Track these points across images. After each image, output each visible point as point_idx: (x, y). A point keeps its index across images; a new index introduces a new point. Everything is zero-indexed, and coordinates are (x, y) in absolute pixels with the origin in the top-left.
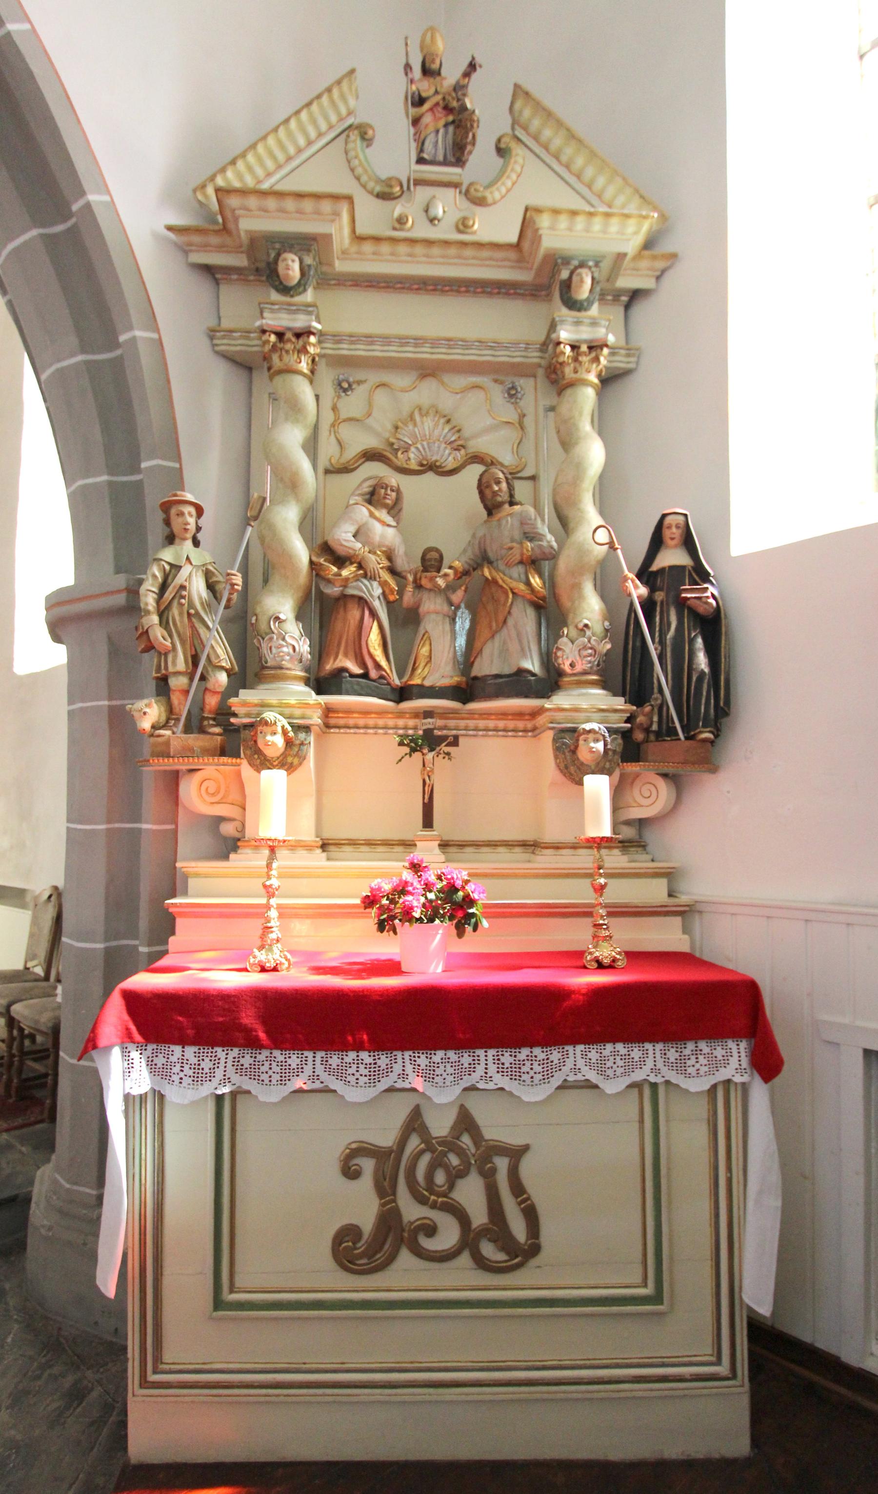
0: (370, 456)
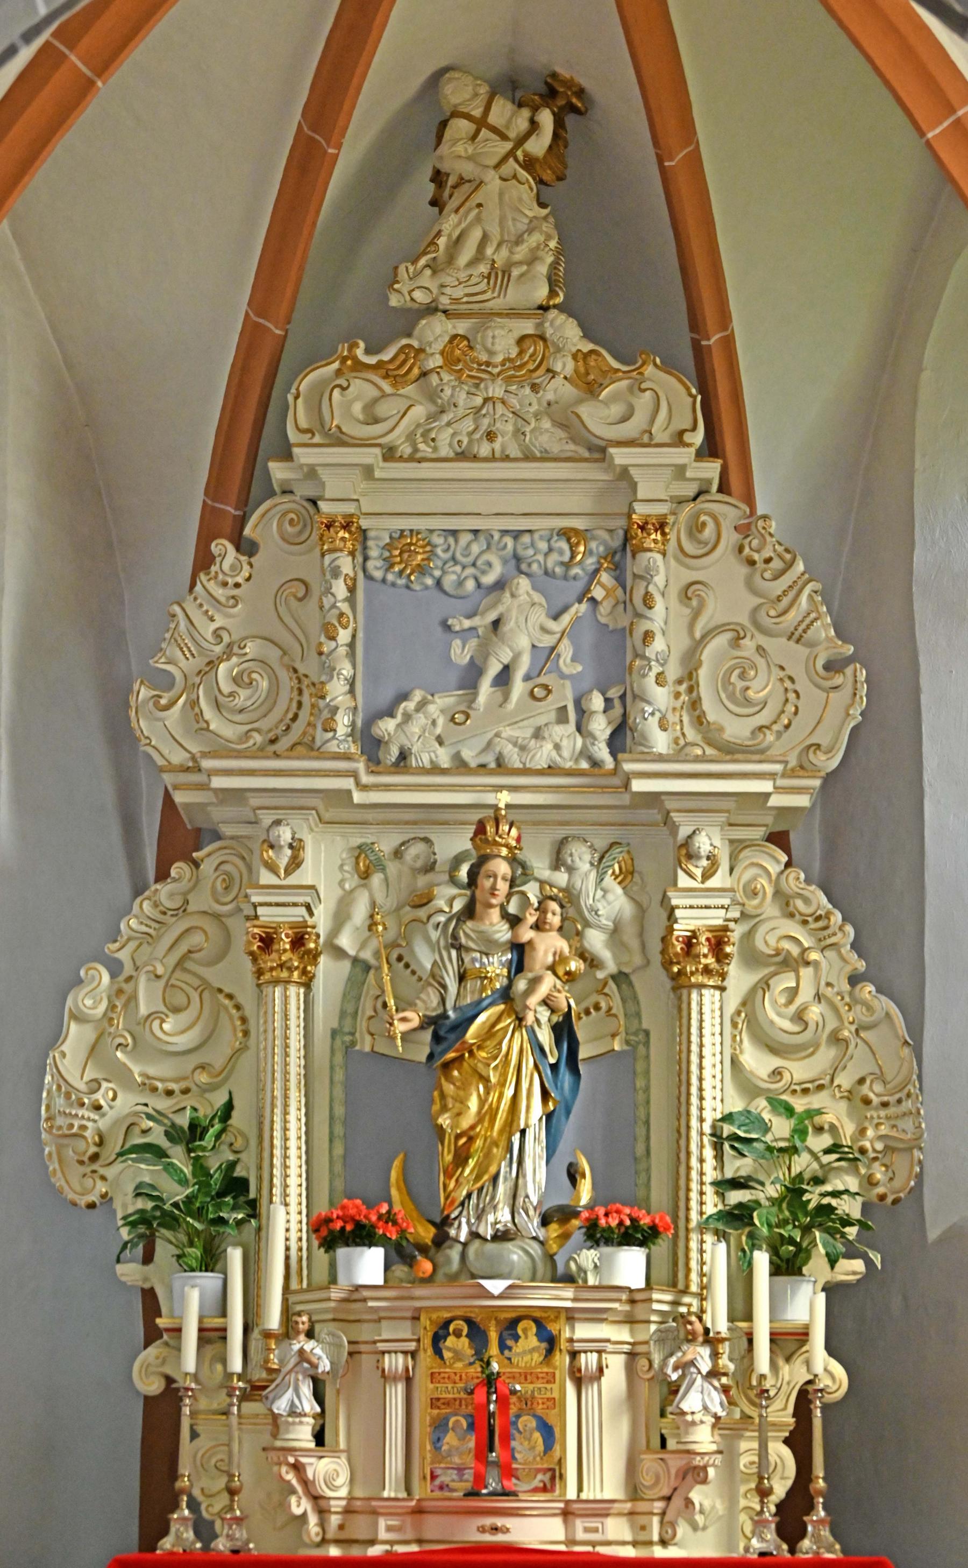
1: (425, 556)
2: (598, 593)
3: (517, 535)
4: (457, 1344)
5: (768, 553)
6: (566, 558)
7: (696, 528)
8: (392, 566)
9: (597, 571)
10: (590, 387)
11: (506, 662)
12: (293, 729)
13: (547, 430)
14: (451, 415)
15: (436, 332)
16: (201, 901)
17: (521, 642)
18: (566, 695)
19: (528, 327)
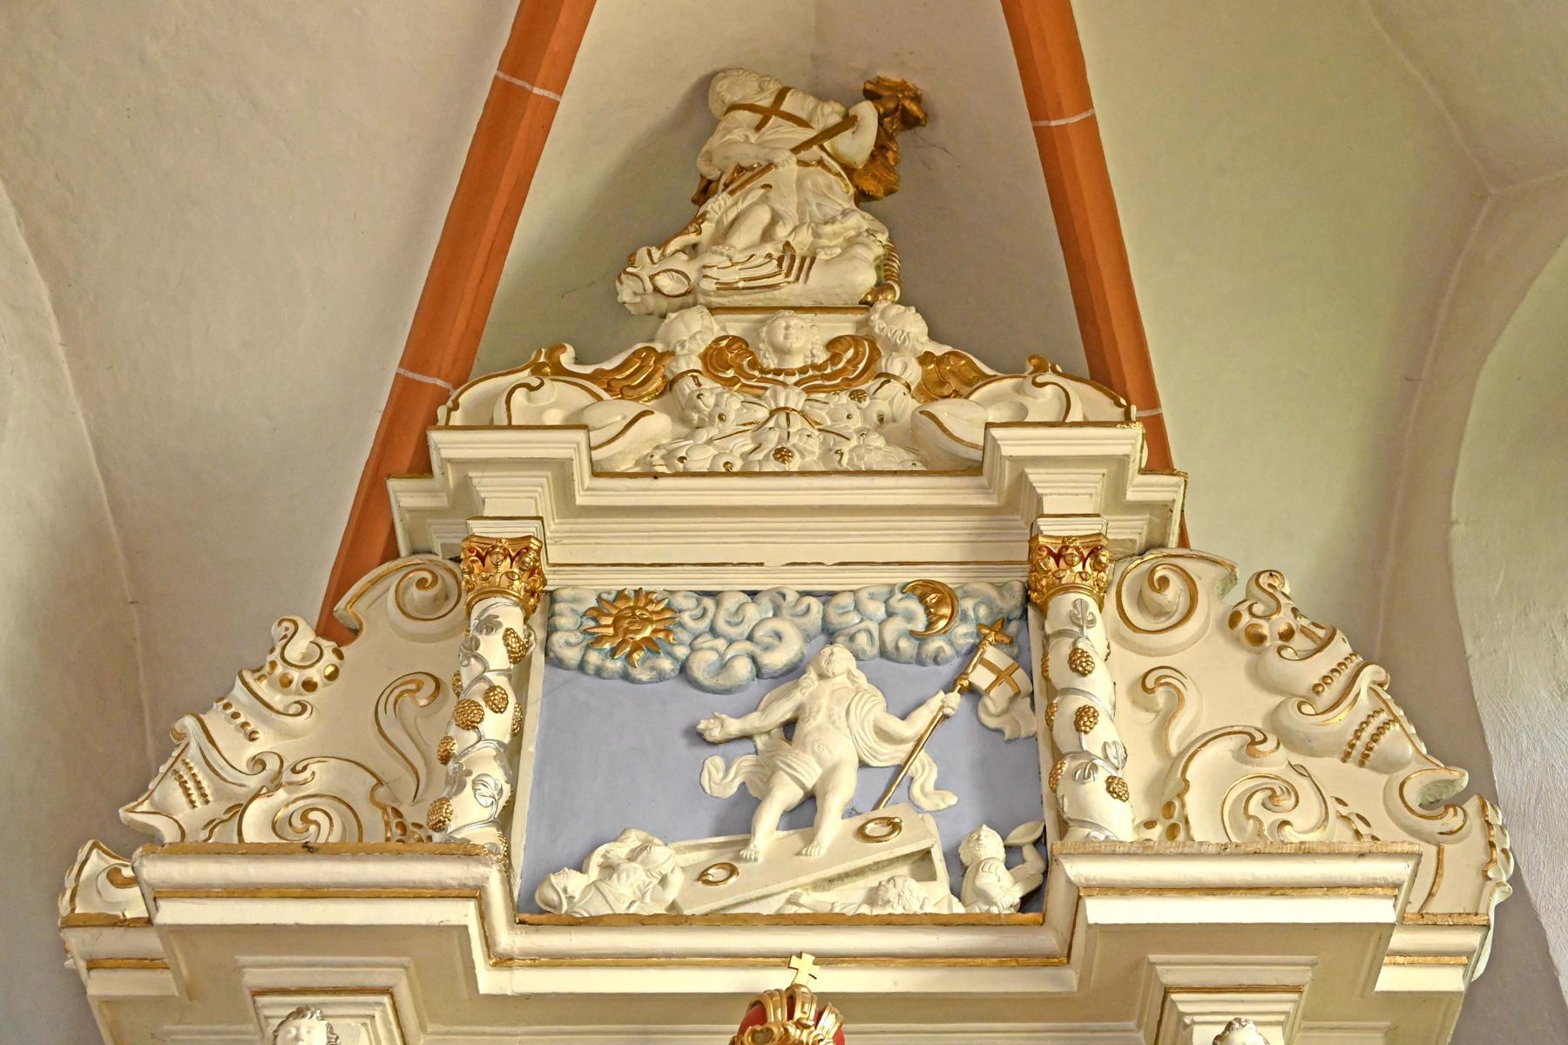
1: (660, 626)
2: (980, 677)
3: (828, 596)
5: (1283, 620)
6: (920, 624)
8: (600, 639)
9: (973, 649)
11: (809, 785)
13: (878, 448)
14: (714, 432)
19: (844, 326)
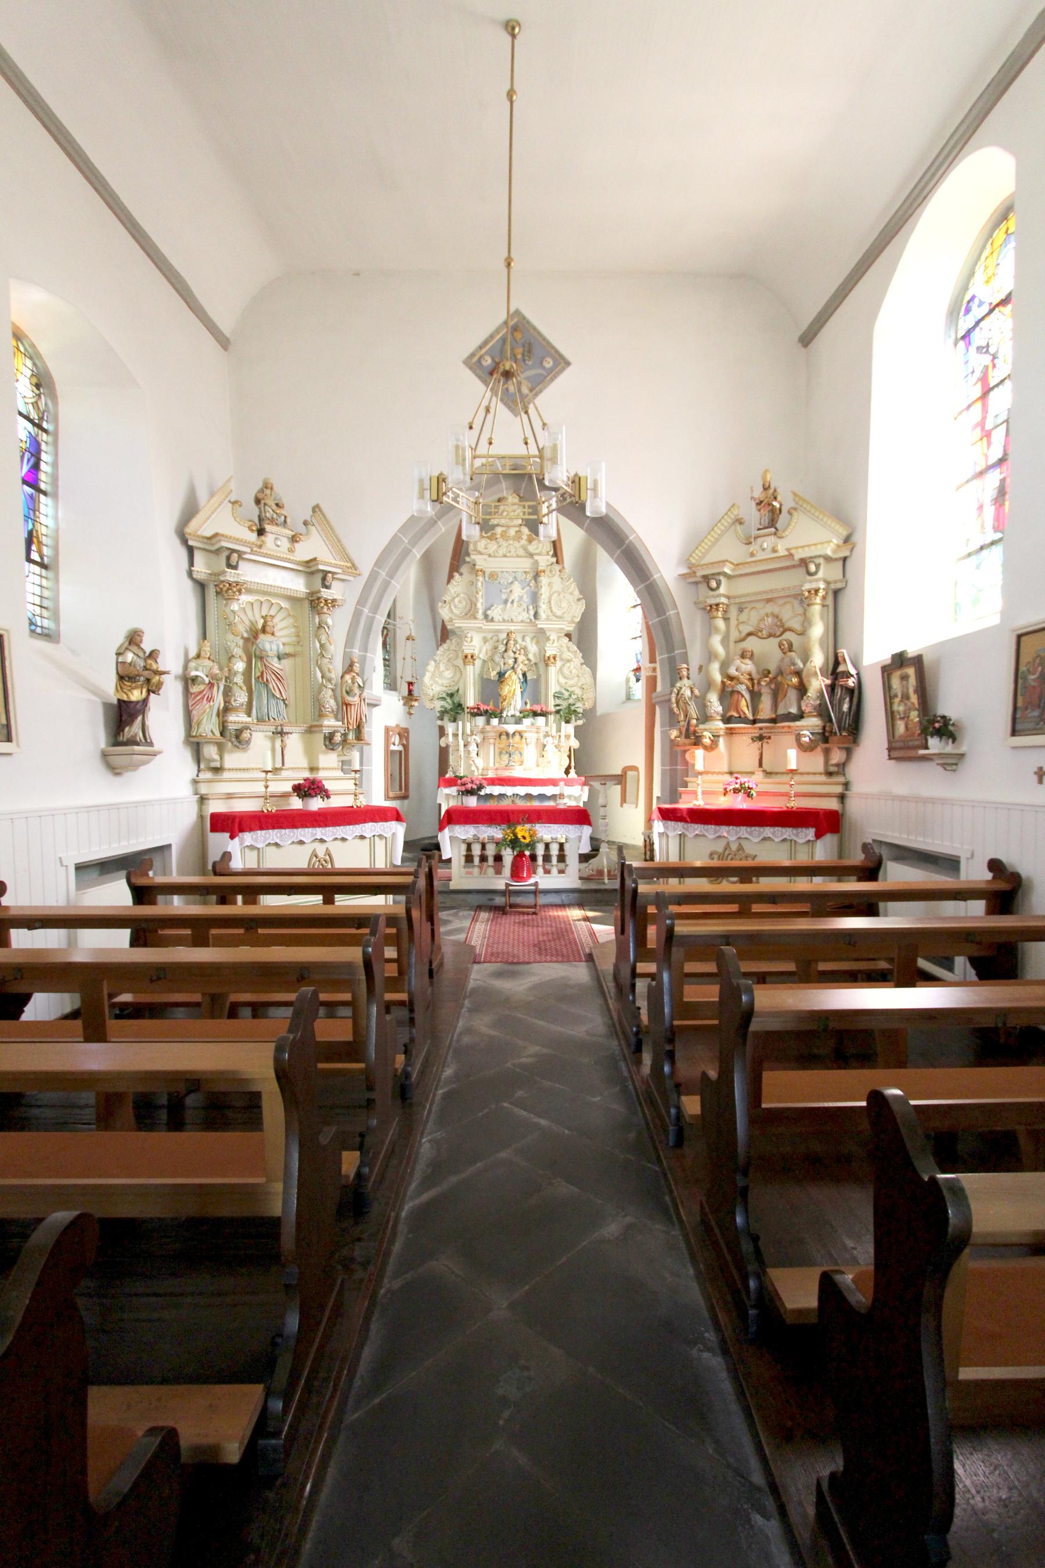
0: (750, 634)
4: (504, 737)
7: (551, 571)
10: (530, 541)
12: (471, 613)
15: (499, 530)
16: (453, 647)
17: (515, 596)
18: (524, 606)
